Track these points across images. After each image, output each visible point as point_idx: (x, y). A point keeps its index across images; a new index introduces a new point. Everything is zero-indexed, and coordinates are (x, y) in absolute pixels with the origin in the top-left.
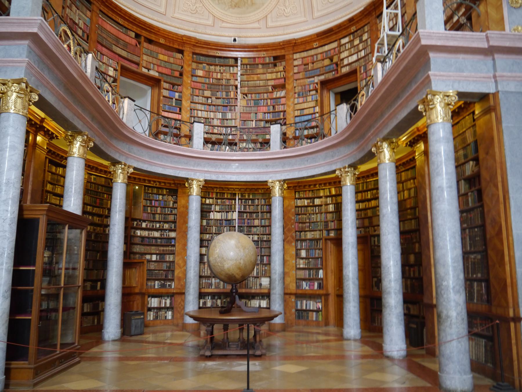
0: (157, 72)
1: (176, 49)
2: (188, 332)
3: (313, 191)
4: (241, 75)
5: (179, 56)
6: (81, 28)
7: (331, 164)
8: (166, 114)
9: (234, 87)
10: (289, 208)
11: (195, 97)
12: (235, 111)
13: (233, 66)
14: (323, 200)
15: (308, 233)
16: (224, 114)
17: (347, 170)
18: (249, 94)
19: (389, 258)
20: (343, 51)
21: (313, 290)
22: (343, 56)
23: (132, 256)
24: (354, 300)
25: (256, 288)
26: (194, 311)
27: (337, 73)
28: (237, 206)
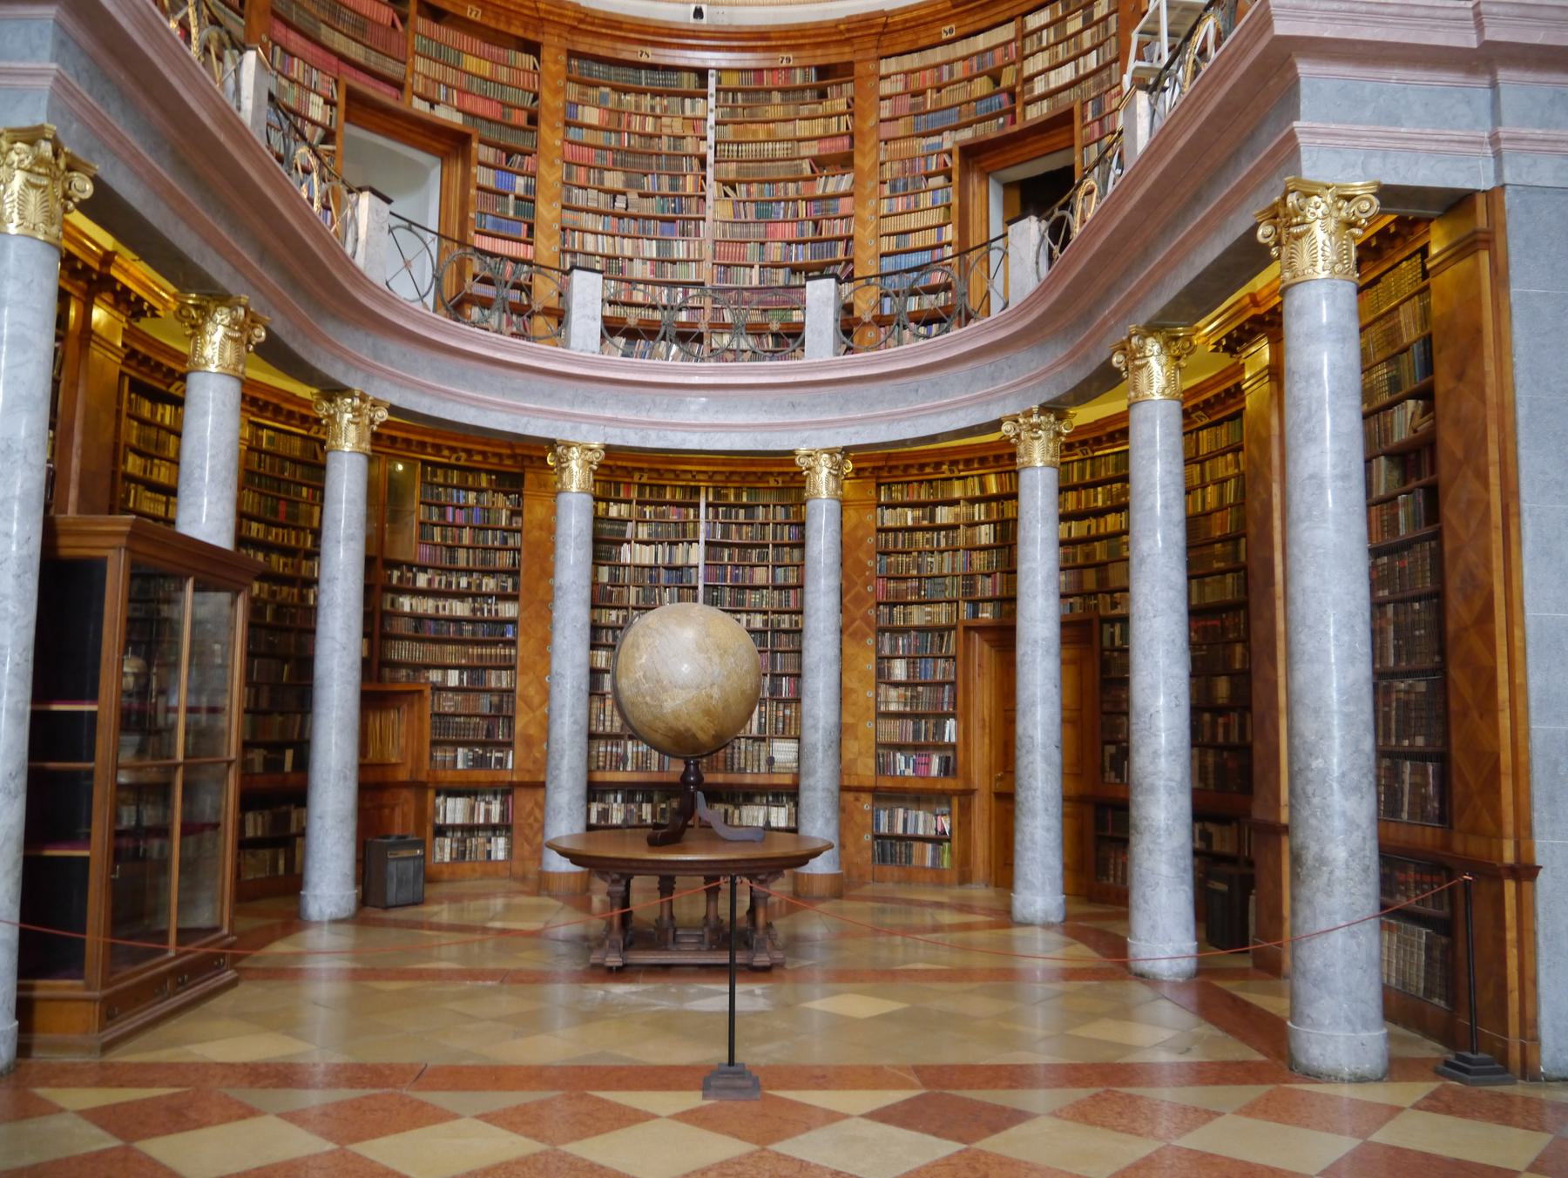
0: (458, 110)
1: (517, 38)
2: (556, 897)
3: (930, 481)
4: (717, 123)
5: (528, 60)
7: (988, 403)
8: (486, 243)
9: (696, 162)
10: (860, 533)
11: (576, 191)
12: (698, 235)
13: (692, 96)
14: (962, 509)
15: (915, 609)
17: (1035, 420)
18: (740, 182)
19: (1154, 687)
20: (1033, 54)
22: (1031, 67)
23: (387, 672)
24: (1046, 810)
25: (756, 770)
26: (572, 837)
27: (1013, 122)
28: (702, 527)
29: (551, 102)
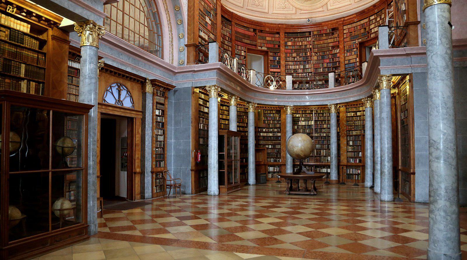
5: (277, 36)
6: (227, 36)
7: (360, 96)
9: (309, 49)
10: (343, 118)
15: (354, 132)
16: (304, 66)
19: (377, 147)
21: (356, 163)
23: (259, 146)
26: (290, 173)
28: (314, 118)
29: (282, 42)
